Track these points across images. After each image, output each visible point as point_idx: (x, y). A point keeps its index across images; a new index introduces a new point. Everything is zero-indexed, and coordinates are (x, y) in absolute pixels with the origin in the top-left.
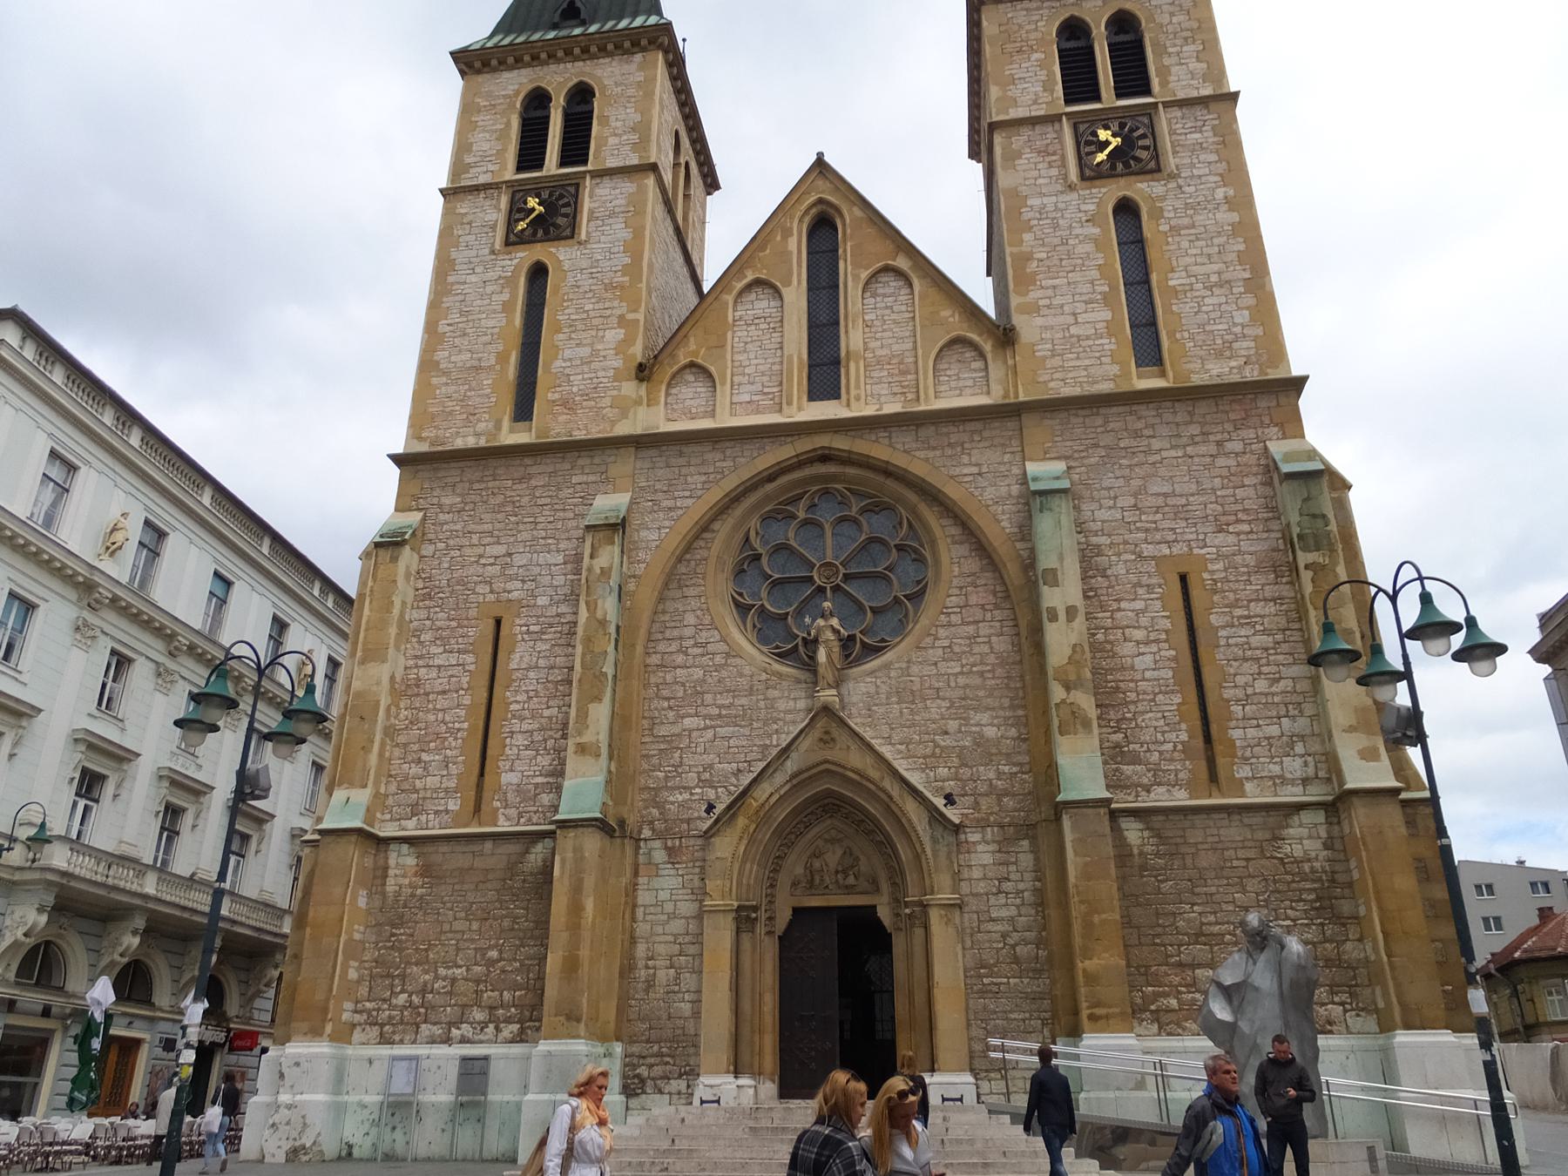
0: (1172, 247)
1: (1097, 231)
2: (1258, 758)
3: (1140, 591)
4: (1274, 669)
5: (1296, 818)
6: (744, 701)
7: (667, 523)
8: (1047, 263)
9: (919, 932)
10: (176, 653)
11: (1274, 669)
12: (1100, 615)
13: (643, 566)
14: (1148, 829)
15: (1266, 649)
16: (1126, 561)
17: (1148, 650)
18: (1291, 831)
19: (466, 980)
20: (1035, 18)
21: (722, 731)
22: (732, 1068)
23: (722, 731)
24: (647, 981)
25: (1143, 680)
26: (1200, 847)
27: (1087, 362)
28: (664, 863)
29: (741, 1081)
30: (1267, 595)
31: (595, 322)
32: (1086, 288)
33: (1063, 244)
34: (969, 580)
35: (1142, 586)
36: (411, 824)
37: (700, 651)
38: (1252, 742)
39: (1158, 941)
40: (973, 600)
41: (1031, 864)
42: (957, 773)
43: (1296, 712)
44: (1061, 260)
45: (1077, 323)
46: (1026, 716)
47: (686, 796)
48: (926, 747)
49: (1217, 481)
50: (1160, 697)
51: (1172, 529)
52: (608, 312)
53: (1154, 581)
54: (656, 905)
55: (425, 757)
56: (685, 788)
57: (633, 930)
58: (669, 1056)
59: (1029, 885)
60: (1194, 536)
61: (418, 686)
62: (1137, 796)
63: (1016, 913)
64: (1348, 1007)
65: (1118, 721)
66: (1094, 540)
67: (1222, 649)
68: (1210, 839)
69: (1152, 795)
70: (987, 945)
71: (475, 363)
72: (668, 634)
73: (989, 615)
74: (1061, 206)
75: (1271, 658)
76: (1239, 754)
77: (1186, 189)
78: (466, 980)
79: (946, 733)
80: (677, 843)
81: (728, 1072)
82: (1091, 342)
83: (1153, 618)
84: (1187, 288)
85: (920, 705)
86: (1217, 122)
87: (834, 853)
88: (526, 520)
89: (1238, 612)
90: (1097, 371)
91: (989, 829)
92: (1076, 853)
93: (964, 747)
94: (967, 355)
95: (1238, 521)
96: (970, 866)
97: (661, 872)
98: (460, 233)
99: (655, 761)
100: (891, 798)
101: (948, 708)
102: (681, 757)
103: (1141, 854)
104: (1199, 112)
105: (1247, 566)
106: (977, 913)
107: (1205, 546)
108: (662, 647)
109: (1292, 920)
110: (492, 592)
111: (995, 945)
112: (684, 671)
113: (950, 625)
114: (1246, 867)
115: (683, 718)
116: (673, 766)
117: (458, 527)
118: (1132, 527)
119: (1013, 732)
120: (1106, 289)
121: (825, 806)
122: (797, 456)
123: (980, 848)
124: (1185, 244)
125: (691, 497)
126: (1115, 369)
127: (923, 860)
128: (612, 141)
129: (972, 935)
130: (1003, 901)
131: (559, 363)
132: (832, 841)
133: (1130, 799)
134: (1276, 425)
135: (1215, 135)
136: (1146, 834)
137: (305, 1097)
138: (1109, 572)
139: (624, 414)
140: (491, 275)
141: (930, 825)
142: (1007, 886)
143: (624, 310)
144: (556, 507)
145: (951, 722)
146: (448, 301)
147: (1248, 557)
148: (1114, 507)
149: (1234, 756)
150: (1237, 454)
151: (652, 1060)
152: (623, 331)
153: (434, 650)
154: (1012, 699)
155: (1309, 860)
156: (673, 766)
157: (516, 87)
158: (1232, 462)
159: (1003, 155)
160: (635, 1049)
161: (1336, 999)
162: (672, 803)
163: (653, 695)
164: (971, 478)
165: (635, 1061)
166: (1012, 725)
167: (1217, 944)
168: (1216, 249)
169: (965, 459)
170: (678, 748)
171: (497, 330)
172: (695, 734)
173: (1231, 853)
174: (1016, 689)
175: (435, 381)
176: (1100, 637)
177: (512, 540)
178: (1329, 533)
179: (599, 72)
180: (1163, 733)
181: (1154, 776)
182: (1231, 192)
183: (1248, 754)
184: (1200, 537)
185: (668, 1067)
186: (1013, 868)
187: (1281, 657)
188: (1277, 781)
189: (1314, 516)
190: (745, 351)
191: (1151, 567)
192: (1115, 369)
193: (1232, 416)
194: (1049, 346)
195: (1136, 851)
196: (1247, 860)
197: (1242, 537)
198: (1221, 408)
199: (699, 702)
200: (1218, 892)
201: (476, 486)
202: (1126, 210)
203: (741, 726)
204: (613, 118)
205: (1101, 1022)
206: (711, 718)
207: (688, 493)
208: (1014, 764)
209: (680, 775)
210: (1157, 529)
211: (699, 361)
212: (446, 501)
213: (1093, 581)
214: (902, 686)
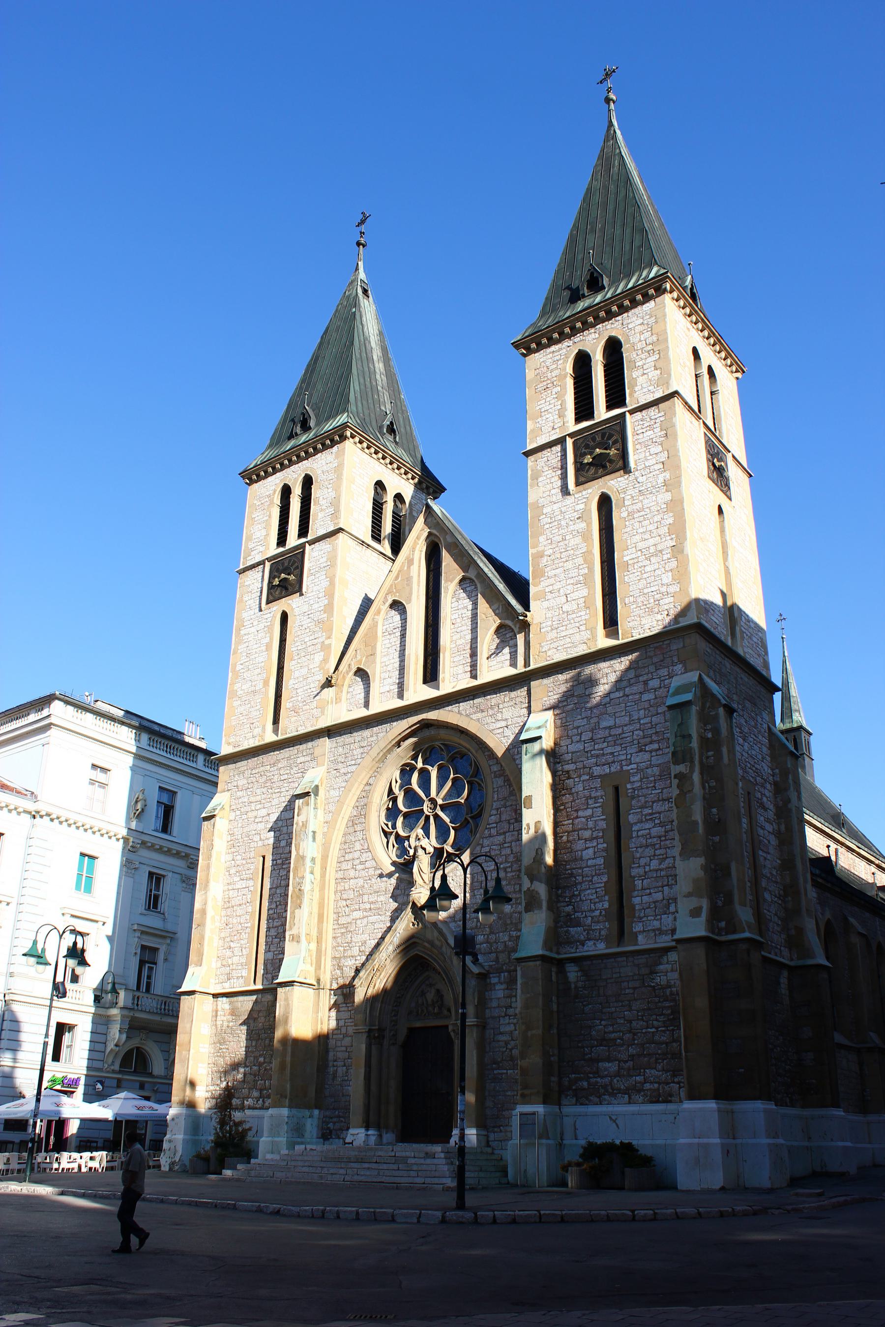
0: (629, 529)
1: (584, 525)
2: (647, 917)
3: (590, 802)
4: (662, 851)
5: (665, 958)
7: (344, 784)
8: (552, 557)
10: (192, 866)
11: (662, 851)
12: (566, 823)
13: (331, 814)
14: (581, 970)
15: (660, 837)
16: (583, 781)
17: (591, 845)
18: (661, 967)
19: (250, 1074)
20: (558, 358)
21: (372, 919)
22: (365, 1124)
23: (372, 919)
24: (333, 1074)
25: (587, 867)
26: (609, 981)
27: (571, 632)
29: (370, 1132)
30: (665, 796)
31: (310, 649)
32: (574, 573)
33: (564, 539)
34: (502, 803)
35: (591, 798)
36: (227, 985)
37: (362, 867)
38: (645, 906)
39: (580, 1045)
40: (504, 817)
42: (488, 937)
43: (673, 882)
44: (561, 553)
45: (567, 601)
48: (473, 922)
49: (642, 712)
50: (595, 878)
51: (612, 753)
52: (316, 641)
53: (598, 794)
55: (232, 945)
57: (327, 1044)
58: (342, 1117)
60: (623, 757)
61: (229, 902)
62: (577, 949)
64: (682, 1085)
65: (570, 898)
66: (567, 768)
67: (633, 840)
68: (614, 976)
69: (586, 948)
70: (498, 1049)
71: (253, 688)
72: (347, 858)
74: (563, 509)
75: (662, 843)
76: (637, 915)
77: (640, 479)
78: (250, 1074)
81: (362, 1127)
82: (574, 616)
83: (596, 821)
84: (636, 561)
86: (662, 419)
88: (276, 791)
89: (647, 811)
90: (577, 638)
91: (502, 974)
92: (522, 992)
94: (508, 636)
95: (651, 743)
96: (491, 999)
98: (246, 599)
103: (576, 987)
104: (652, 412)
105: (654, 776)
106: (494, 1029)
107: (631, 764)
108: (344, 866)
109: (657, 1028)
110: (261, 839)
111: (501, 1049)
113: (490, 836)
114: (633, 993)
117: (246, 800)
118: (589, 755)
120: (586, 571)
122: (410, 727)
123: (497, 987)
124: (637, 525)
125: (355, 765)
126: (586, 635)
128: (320, 515)
130: (507, 1021)
131: (291, 682)
132: (431, 985)
133: (573, 951)
134: (681, 662)
135: (661, 430)
136: (579, 974)
137: (176, 1136)
138: (573, 790)
139: (323, 713)
140: (262, 626)
143: (324, 638)
144: (290, 780)
146: (242, 647)
147: (655, 769)
148: (580, 741)
149: (634, 917)
150: (655, 689)
151: (335, 1120)
152: (322, 653)
153: (236, 879)
155: (670, 987)
157: (273, 488)
158: (652, 696)
159: (531, 475)
160: (328, 1113)
161: (676, 1080)
164: (502, 730)
165: (327, 1120)
167: (612, 1046)
168: (656, 524)
169: (499, 716)
170: (350, 931)
171: (263, 664)
172: (359, 922)
173: (626, 984)
175: (236, 704)
176: (565, 838)
177: (269, 804)
178: (691, 748)
179: (315, 466)
180: (595, 903)
181: (588, 933)
182: (668, 477)
183: (642, 915)
184: (629, 757)
185: (342, 1124)
187: (668, 842)
188: (657, 932)
189: (683, 737)
190: (388, 655)
191: (597, 783)
192: (586, 635)
193: (655, 660)
194: (550, 623)
195: (573, 986)
196: (634, 988)
197: (654, 754)
198: (648, 654)
200: (616, 1012)
201: (254, 771)
202: (605, 503)
204: (321, 499)
205: (526, 1099)
206: (365, 910)
207: (353, 762)
210: (603, 755)
211: (362, 667)
212: (242, 782)
213: (564, 798)
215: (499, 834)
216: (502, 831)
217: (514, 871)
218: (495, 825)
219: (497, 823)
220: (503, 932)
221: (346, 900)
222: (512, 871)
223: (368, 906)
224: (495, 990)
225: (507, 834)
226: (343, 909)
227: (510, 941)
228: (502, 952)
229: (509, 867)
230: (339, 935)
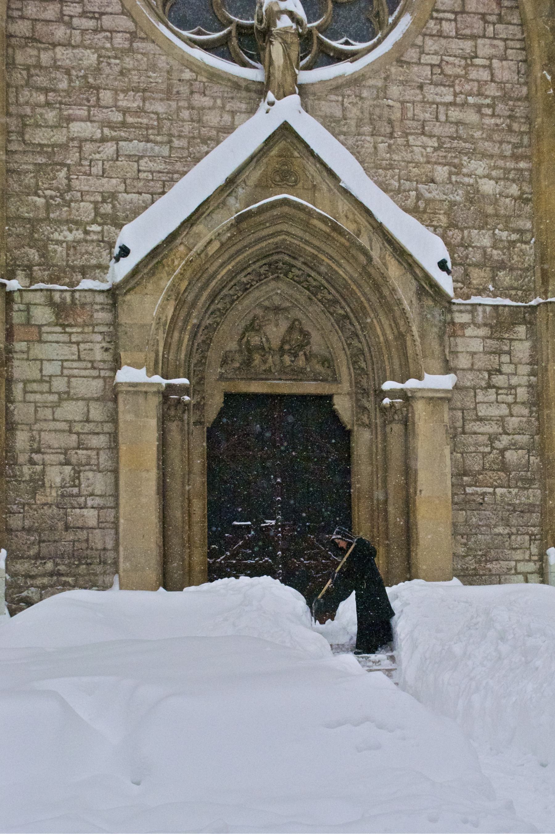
6: (160, 108)
9: (397, 428)
28: (49, 325)
37: (91, 24)
41: (527, 354)
46: (531, 170)
47: (79, 235)
54: (41, 381)
56: (76, 223)
57: (8, 413)
59: (524, 380)
63: (507, 412)
73: (490, 30)
79: (433, 181)
80: (68, 300)
85: (400, 141)
87: (277, 325)
93: (453, 204)
97: (45, 337)
99: (29, 180)
100: (370, 259)
101: (436, 149)
102: (69, 179)
112: (69, 52)
113: (440, 35)
115: (70, 119)
116: (58, 189)
119: (514, 190)
121: (270, 264)
123: (469, 332)
127: (409, 343)
129: (455, 436)
141: (420, 300)
142: (500, 380)
145: (439, 168)
154: (515, 146)
156: (58, 189)
162: (58, 242)
163: (23, 83)
166: (514, 181)
170: (63, 165)
172: (88, 147)
174: (522, 133)
186: (505, 358)
199: (93, 99)
203: (156, 143)
206: (111, 126)
208: (514, 231)
209: (68, 204)
214: (377, 111)
215: (459, 36)
216: (468, 32)
217: (499, 116)
218: (452, 16)
219: (456, 13)
220: (481, 228)
221: (39, 89)
222: (493, 115)
223: (117, 117)
224: (464, 336)
225: (480, 41)
226: (38, 110)
227: (494, 247)
228: (476, 265)
229: (488, 106)
230: (31, 167)
